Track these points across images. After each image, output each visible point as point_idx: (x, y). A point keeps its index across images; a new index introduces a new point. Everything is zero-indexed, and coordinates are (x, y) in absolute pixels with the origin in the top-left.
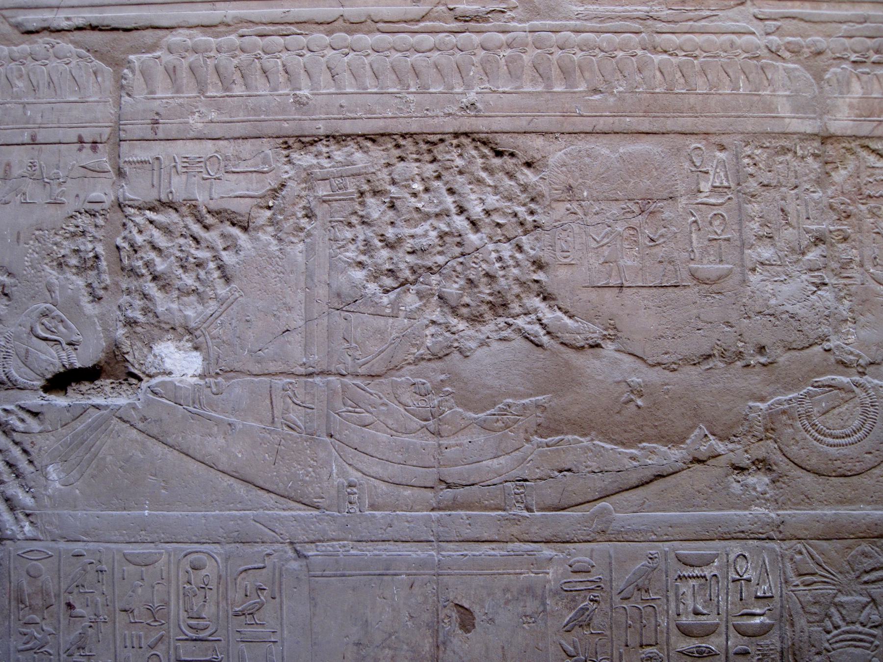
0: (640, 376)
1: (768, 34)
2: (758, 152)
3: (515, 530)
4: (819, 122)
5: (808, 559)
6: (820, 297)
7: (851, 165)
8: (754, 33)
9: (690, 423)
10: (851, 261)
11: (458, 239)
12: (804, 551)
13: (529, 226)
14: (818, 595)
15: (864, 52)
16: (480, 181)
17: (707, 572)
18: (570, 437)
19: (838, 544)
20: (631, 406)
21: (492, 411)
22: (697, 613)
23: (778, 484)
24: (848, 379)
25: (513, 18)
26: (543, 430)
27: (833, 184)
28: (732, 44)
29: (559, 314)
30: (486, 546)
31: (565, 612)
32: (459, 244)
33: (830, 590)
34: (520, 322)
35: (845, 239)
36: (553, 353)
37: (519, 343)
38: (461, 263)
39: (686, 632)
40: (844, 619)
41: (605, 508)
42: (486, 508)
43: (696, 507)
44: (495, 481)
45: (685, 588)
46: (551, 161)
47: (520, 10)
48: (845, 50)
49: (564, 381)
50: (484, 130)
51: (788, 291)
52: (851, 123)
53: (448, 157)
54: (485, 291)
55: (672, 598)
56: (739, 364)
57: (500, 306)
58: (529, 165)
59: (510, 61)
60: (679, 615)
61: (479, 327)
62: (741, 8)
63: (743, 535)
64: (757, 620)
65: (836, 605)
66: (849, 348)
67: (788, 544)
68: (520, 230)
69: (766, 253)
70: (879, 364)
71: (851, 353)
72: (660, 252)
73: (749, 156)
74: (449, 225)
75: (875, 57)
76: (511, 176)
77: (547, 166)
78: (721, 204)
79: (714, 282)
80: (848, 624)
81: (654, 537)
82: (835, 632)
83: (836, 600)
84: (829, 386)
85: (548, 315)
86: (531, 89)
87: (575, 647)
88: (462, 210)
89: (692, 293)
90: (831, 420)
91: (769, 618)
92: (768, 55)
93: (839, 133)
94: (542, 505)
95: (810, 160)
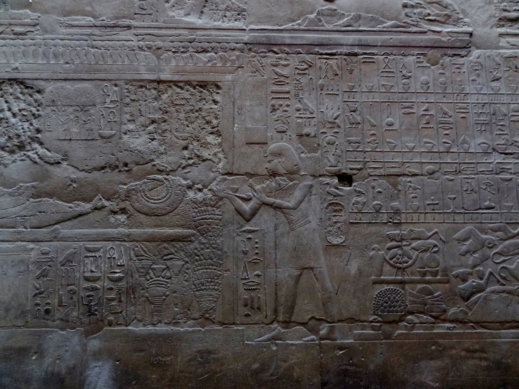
0: (76, 175)
1: (139, 41)
2: (130, 87)
3: (19, 236)
4: (156, 75)
5: (141, 250)
6: (152, 144)
7: (170, 92)
8: (133, 41)
9: (95, 194)
10: (167, 130)
11: (7, 121)
12: (139, 246)
13: (36, 116)
14: (144, 265)
15: (178, 48)
16: (18, 98)
17: (97, 255)
18: (45, 199)
19: (154, 244)
20: (71, 187)
21: (15, 188)
22: (92, 271)
23: (130, 219)
24: (162, 177)
25: (37, 34)
26: (34, 196)
27: (162, 99)
28: (124, 45)
29: (45, 150)
30: (7, 243)
31: (37, 270)
32: (7, 123)
33: (150, 262)
34: (29, 153)
35: (165, 121)
36: (41, 166)
37: (28, 161)
38: (7, 130)
39: (87, 279)
40: (155, 275)
41: (58, 228)
42: (8, 228)
43: (96, 228)
44: (13, 217)
45: (87, 261)
46: (47, 90)
47: (40, 31)
48: (171, 47)
49: (45, 176)
50: (21, 78)
51: (139, 142)
52: (170, 76)
53: (6, 88)
54: (16, 141)
55: (82, 265)
56: (117, 170)
57: (21, 147)
58: (39, 92)
59: (35, 51)
60: (84, 272)
61: (13, 155)
62: (129, 31)
63: (113, 239)
64: (117, 275)
65: (152, 269)
66: (163, 164)
67: (133, 243)
68: (33, 117)
69: (131, 126)
70: (175, 171)
71: (163, 166)
72: (87, 126)
73: (127, 89)
74: (3, 115)
75: (182, 50)
76: (31, 96)
77: (45, 92)
78: (114, 108)
79: (109, 138)
80: (157, 277)
81: (76, 240)
82: (151, 280)
83: (152, 267)
84: (153, 179)
85: (41, 151)
86: (41, 62)
87: (40, 286)
88: (10, 110)
89: (100, 142)
90: (153, 193)
91: (123, 274)
92: (139, 49)
93: (165, 80)
94: (31, 226)
95: (152, 90)
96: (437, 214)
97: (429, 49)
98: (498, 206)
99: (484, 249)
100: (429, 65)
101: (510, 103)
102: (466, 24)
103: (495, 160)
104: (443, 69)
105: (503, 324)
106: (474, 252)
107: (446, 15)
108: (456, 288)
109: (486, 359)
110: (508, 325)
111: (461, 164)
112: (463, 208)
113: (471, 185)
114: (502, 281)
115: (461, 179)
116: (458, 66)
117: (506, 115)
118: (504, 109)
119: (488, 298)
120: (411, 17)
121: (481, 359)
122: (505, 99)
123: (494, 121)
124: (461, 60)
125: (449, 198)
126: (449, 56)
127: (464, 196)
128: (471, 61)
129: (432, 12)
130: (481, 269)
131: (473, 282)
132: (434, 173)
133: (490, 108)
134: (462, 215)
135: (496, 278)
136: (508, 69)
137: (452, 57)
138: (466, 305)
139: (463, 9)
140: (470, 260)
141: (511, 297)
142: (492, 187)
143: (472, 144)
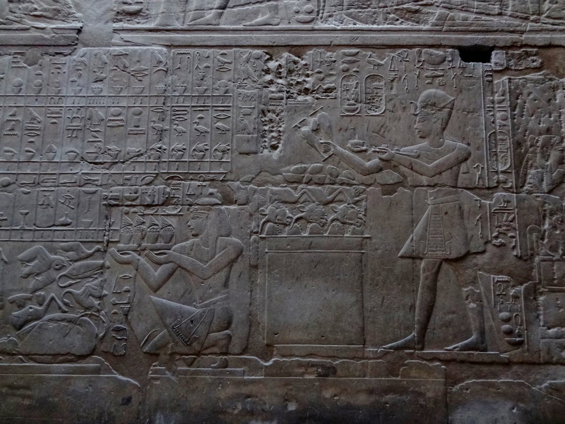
96: (4, 232)
97: (29, 47)
98: (74, 223)
99: (50, 271)
100: (25, 65)
101: (110, 107)
102: (78, 20)
103: (81, 170)
104: (41, 70)
105: (56, 357)
106: (38, 275)
107: (55, 10)
108: (11, 314)
109: (29, 397)
110: (61, 358)
111: (42, 176)
112: (35, 225)
113: (49, 199)
114: (64, 308)
115: (38, 191)
116: (59, 66)
117: (102, 120)
118: (101, 114)
119: (44, 327)
120: (15, 13)
121: (24, 397)
122: (105, 102)
123: (88, 127)
124: (63, 59)
125: (22, 214)
126: (50, 55)
127: (38, 211)
128: (74, 60)
129: (40, 7)
130: (43, 293)
131: (32, 307)
132: (9, 185)
133: (86, 111)
134: (32, 232)
135: (58, 304)
136: (115, 68)
137: (54, 56)
138: (17, 335)
139: (78, 3)
140: (32, 283)
141: (71, 325)
142: (73, 201)
143: (59, 154)
